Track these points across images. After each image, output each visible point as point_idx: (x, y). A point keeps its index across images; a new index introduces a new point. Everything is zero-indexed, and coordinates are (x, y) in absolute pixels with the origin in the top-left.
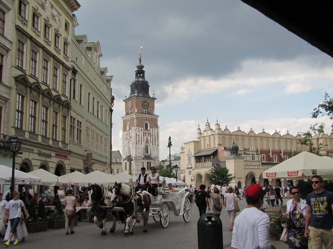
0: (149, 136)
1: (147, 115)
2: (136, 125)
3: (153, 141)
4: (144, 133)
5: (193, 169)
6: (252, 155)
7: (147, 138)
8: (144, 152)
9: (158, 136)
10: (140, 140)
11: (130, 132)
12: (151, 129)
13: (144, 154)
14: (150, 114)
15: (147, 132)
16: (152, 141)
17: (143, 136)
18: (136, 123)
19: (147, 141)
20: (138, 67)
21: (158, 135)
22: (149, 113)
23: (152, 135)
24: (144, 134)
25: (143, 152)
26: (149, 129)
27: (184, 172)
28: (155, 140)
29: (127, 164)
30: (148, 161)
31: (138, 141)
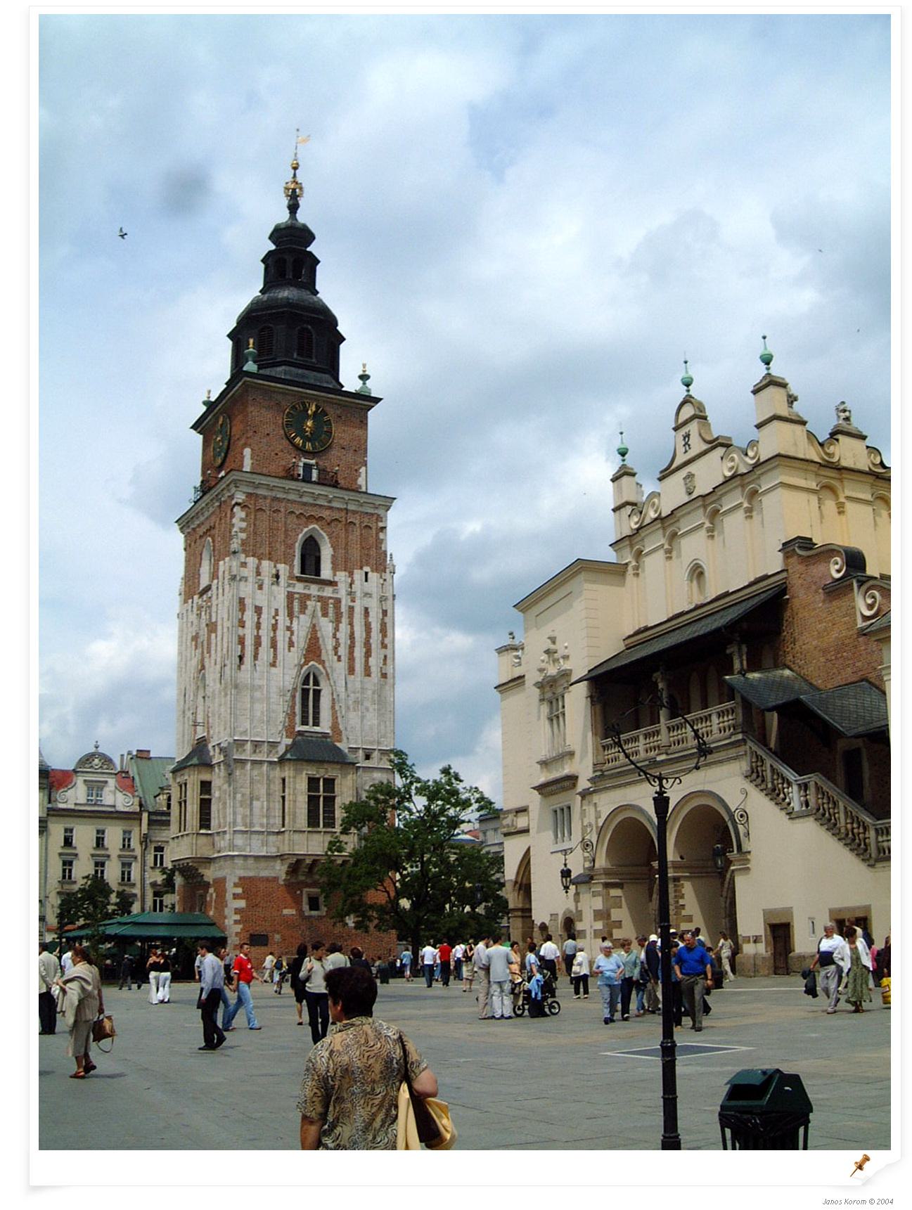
0: (325, 614)
1: (318, 490)
2: (244, 543)
3: (352, 647)
4: (290, 596)
5: (583, 784)
7: (314, 629)
10: (265, 641)
12: (341, 576)
13: (289, 730)
14: (335, 485)
15: (314, 590)
16: (343, 651)
18: (243, 536)
19: (313, 649)
20: (278, 235)
21: (385, 613)
22: (328, 480)
23: (344, 609)
24: (295, 604)
25: (281, 717)
26: (326, 572)
27: (521, 822)
28: (367, 644)
29: (185, 796)
30: (312, 771)
31: (249, 642)
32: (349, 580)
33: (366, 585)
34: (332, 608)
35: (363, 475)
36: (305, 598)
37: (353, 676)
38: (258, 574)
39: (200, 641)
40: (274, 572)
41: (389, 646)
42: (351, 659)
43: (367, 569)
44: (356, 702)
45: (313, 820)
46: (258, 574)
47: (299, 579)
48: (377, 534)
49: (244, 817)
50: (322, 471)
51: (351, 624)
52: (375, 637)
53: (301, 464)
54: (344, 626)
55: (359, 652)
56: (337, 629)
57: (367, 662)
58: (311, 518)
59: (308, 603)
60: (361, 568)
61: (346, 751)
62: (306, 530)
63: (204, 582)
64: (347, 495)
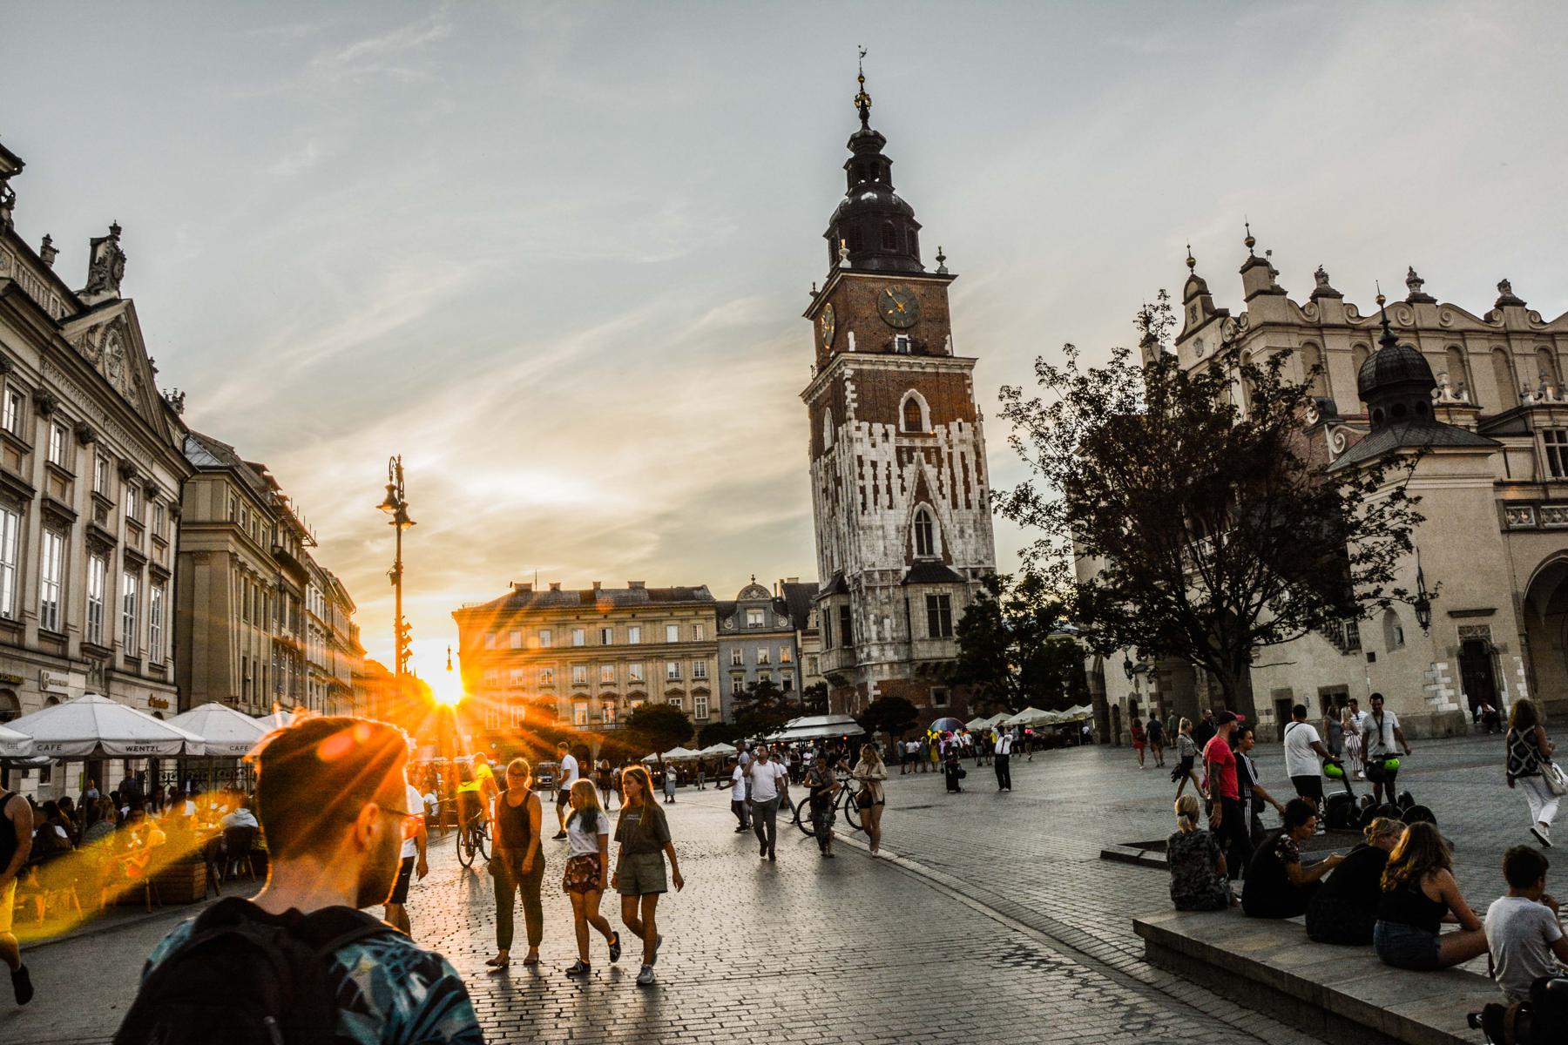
4: (899, 450)
6: (1548, 436)
8: (909, 547)
9: (982, 460)
10: (883, 489)
11: (833, 453)
12: (940, 429)
13: (908, 559)
14: (927, 354)
15: (918, 443)
16: (947, 490)
17: (894, 465)
18: (855, 405)
19: (922, 492)
22: (920, 350)
23: (944, 455)
24: (904, 456)
25: (903, 551)
26: (927, 427)
30: (928, 590)
32: (946, 431)
33: (958, 431)
34: (932, 454)
35: (949, 342)
36: (911, 450)
37: (956, 511)
38: (871, 434)
39: (830, 491)
40: (883, 431)
41: (985, 482)
42: (954, 496)
43: (960, 420)
44: (962, 531)
45: (934, 632)
46: (871, 434)
47: (905, 435)
48: (965, 391)
49: (879, 633)
50: (913, 342)
51: (951, 466)
52: (973, 476)
53: (896, 340)
54: (946, 470)
55: (960, 489)
56: (940, 473)
57: (967, 497)
58: (911, 384)
59: (914, 454)
60: (955, 420)
61: (956, 571)
62: (906, 394)
63: (827, 444)
64: (937, 361)
